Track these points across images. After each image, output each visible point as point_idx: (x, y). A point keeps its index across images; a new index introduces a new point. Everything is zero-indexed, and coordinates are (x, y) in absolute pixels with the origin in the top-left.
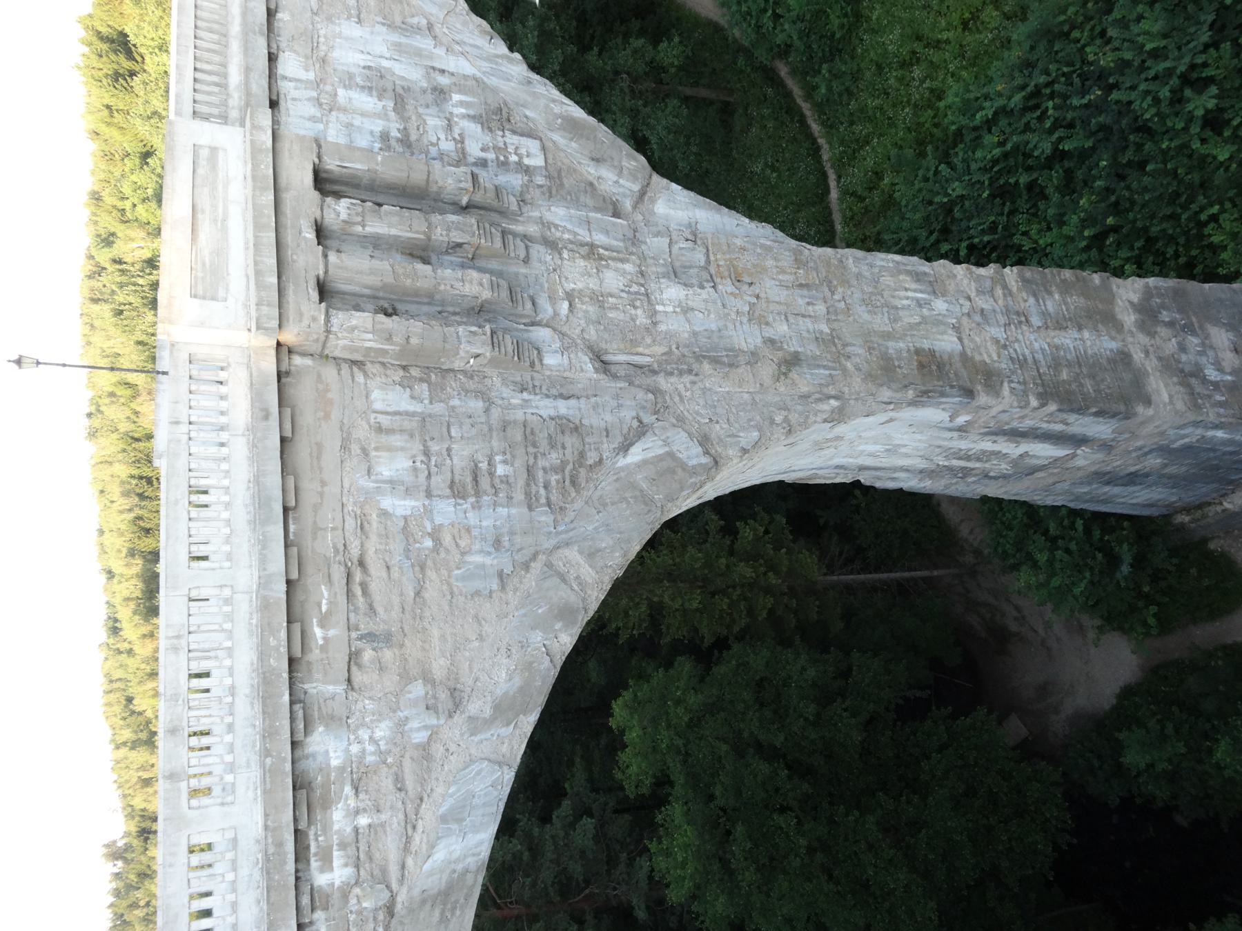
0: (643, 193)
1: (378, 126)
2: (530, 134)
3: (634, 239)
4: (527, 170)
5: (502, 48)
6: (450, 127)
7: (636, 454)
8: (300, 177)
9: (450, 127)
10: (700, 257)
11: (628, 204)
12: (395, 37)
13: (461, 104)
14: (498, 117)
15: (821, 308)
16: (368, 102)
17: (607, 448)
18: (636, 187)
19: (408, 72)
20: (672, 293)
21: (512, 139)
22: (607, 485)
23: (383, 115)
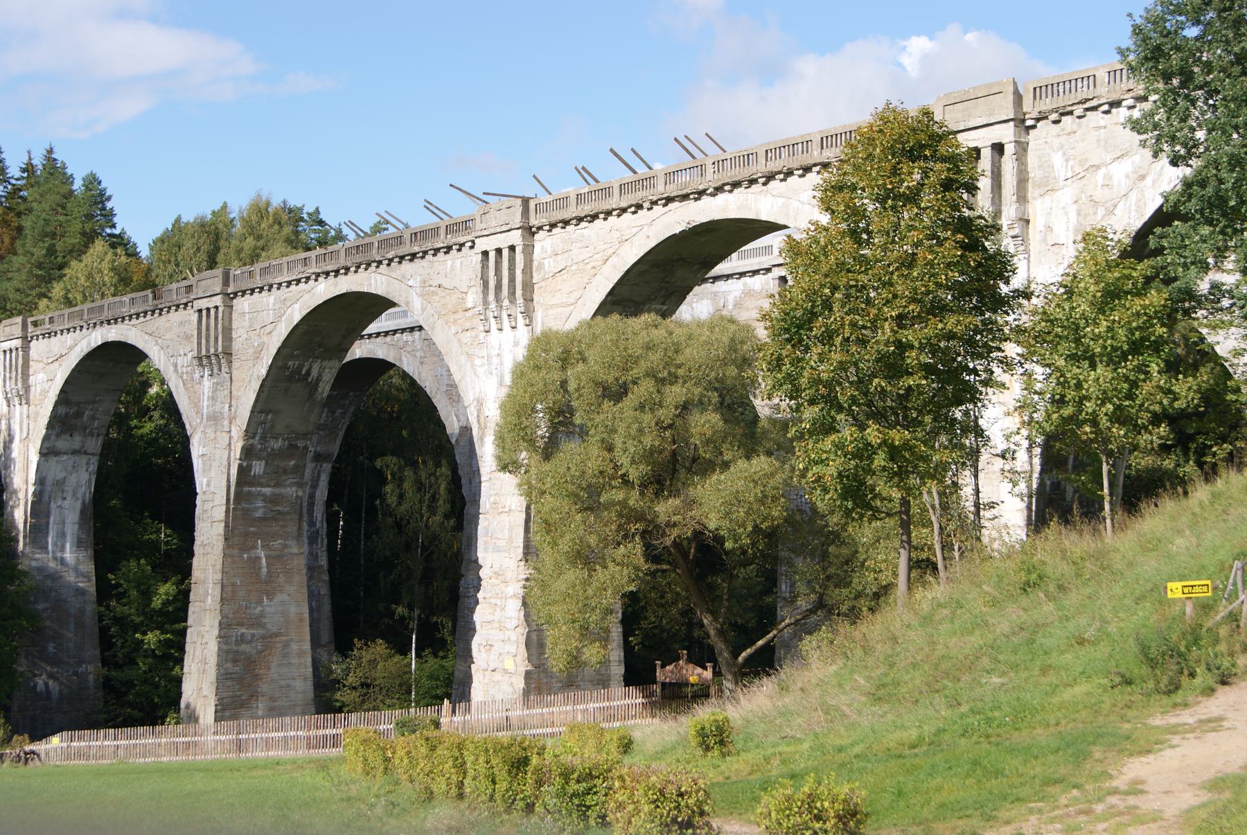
22: (449, 408)
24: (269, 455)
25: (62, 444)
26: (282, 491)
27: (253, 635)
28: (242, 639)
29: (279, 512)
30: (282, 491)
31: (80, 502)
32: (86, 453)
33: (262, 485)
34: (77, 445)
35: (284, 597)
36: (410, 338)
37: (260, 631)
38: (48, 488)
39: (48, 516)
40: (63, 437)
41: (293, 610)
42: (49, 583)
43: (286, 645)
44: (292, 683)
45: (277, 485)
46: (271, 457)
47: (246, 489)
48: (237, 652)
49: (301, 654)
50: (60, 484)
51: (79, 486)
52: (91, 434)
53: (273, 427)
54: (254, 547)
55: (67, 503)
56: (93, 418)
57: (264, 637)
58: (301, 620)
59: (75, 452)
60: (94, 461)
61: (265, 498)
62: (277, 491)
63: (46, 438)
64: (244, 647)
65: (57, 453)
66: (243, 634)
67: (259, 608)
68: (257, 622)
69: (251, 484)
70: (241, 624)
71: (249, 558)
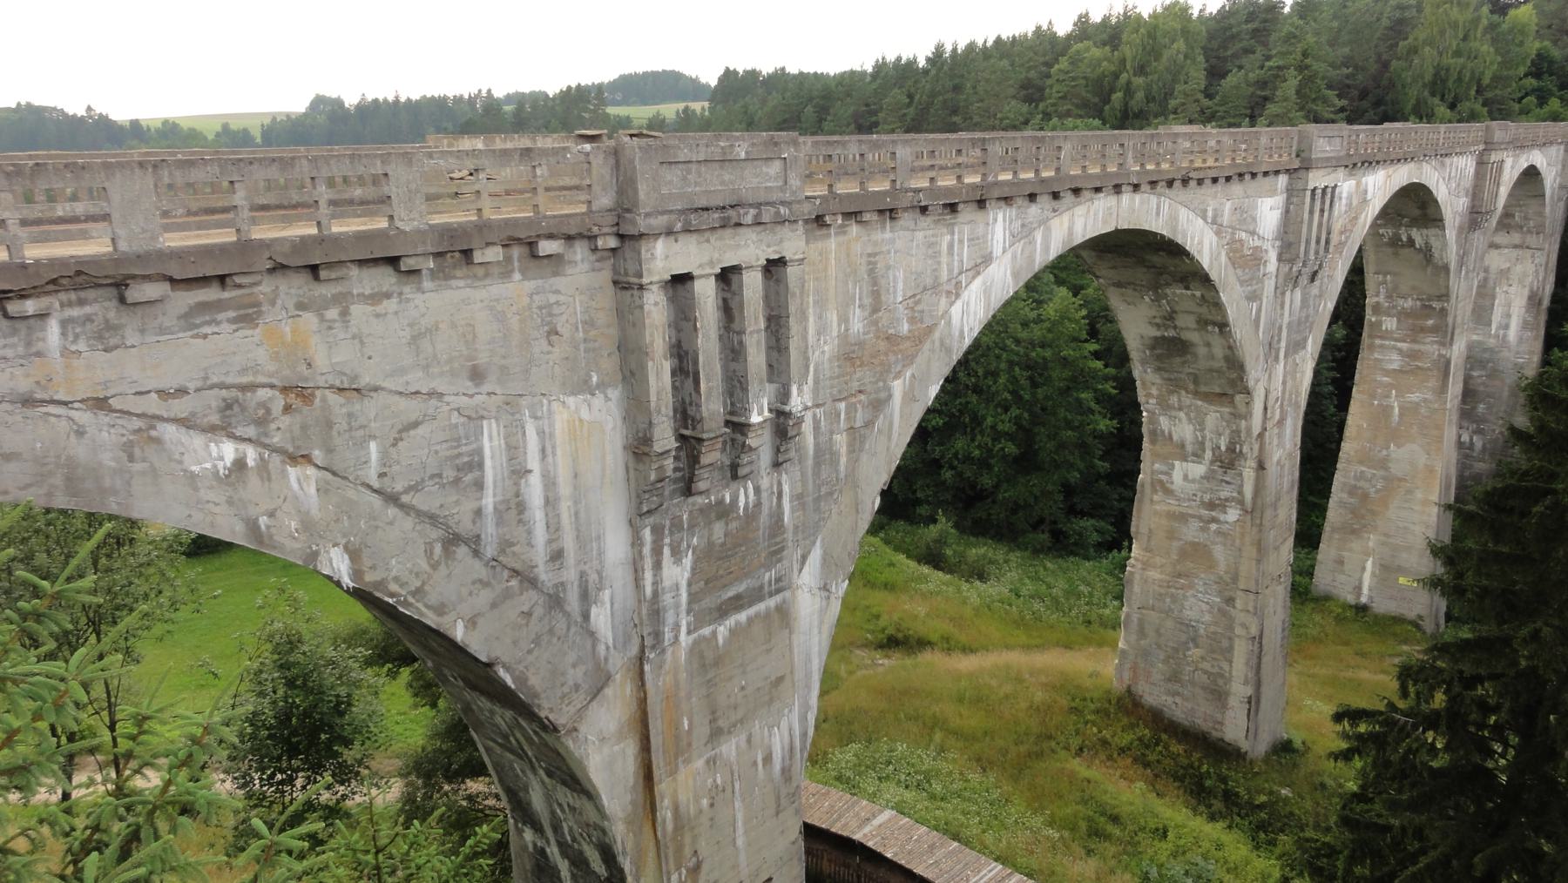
24: (1400, 313)
25: (1501, 238)
26: (1422, 347)
28: (1362, 476)
29: (1419, 368)
30: (1422, 347)
35: (1415, 447)
37: (1382, 473)
38: (1492, 276)
39: (1493, 297)
41: (1422, 460)
42: (1486, 355)
43: (1409, 492)
44: (1412, 527)
45: (1414, 341)
46: (1403, 315)
47: (1378, 342)
49: (1425, 502)
50: (1504, 273)
51: (1525, 275)
52: (1529, 232)
53: (1395, 288)
54: (1388, 396)
55: (1512, 290)
56: (1526, 218)
57: (1384, 478)
59: (1516, 247)
61: (1400, 351)
62: (1416, 347)
65: (1497, 247)
68: (1383, 464)
69: (1382, 338)
70: (1361, 462)
71: (1380, 405)
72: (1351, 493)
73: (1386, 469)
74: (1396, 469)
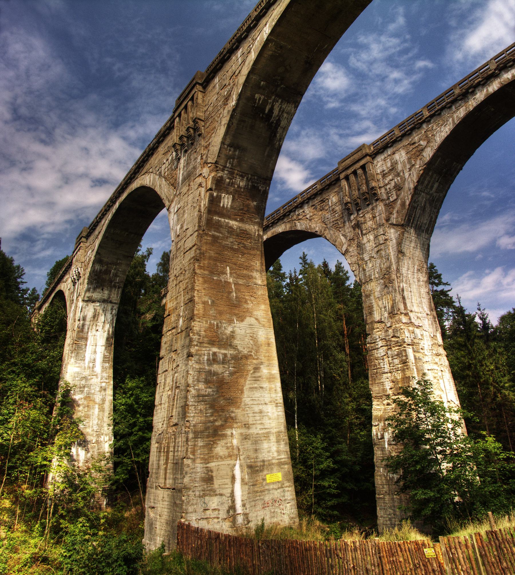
0: (394, 225)
1: (385, 168)
2: (398, 196)
3: (381, 225)
4: (388, 199)
5: (415, 181)
6: (391, 180)
7: (342, 238)
8: (362, 163)
9: (391, 180)
10: (382, 242)
11: (390, 222)
12: (406, 161)
13: (398, 180)
14: (398, 188)
15: (377, 276)
16: (389, 164)
17: (342, 232)
18: (394, 223)
19: (400, 167)
20: (372, 237)
21: (394, 193)
23: (388, 168)
25: (96, 295)
27: (225, 355)
31: (106, 333)
32: (111, 302)
33: (229, 218)
34: (106, 297)
35: (252, 320)
36: (301, 211)
37: (230, 352)
40: (98, 290)
48: (210, 372)
58: (269, 345)
60: (116, 307)
63: (88, 290)
64: (216, 368)
65: (94, 302)
66: (214, 354)
67: (230, 329)
70: (212, 343)
72: (207, 382)
73: (235, 348)
74: (242, 344)
